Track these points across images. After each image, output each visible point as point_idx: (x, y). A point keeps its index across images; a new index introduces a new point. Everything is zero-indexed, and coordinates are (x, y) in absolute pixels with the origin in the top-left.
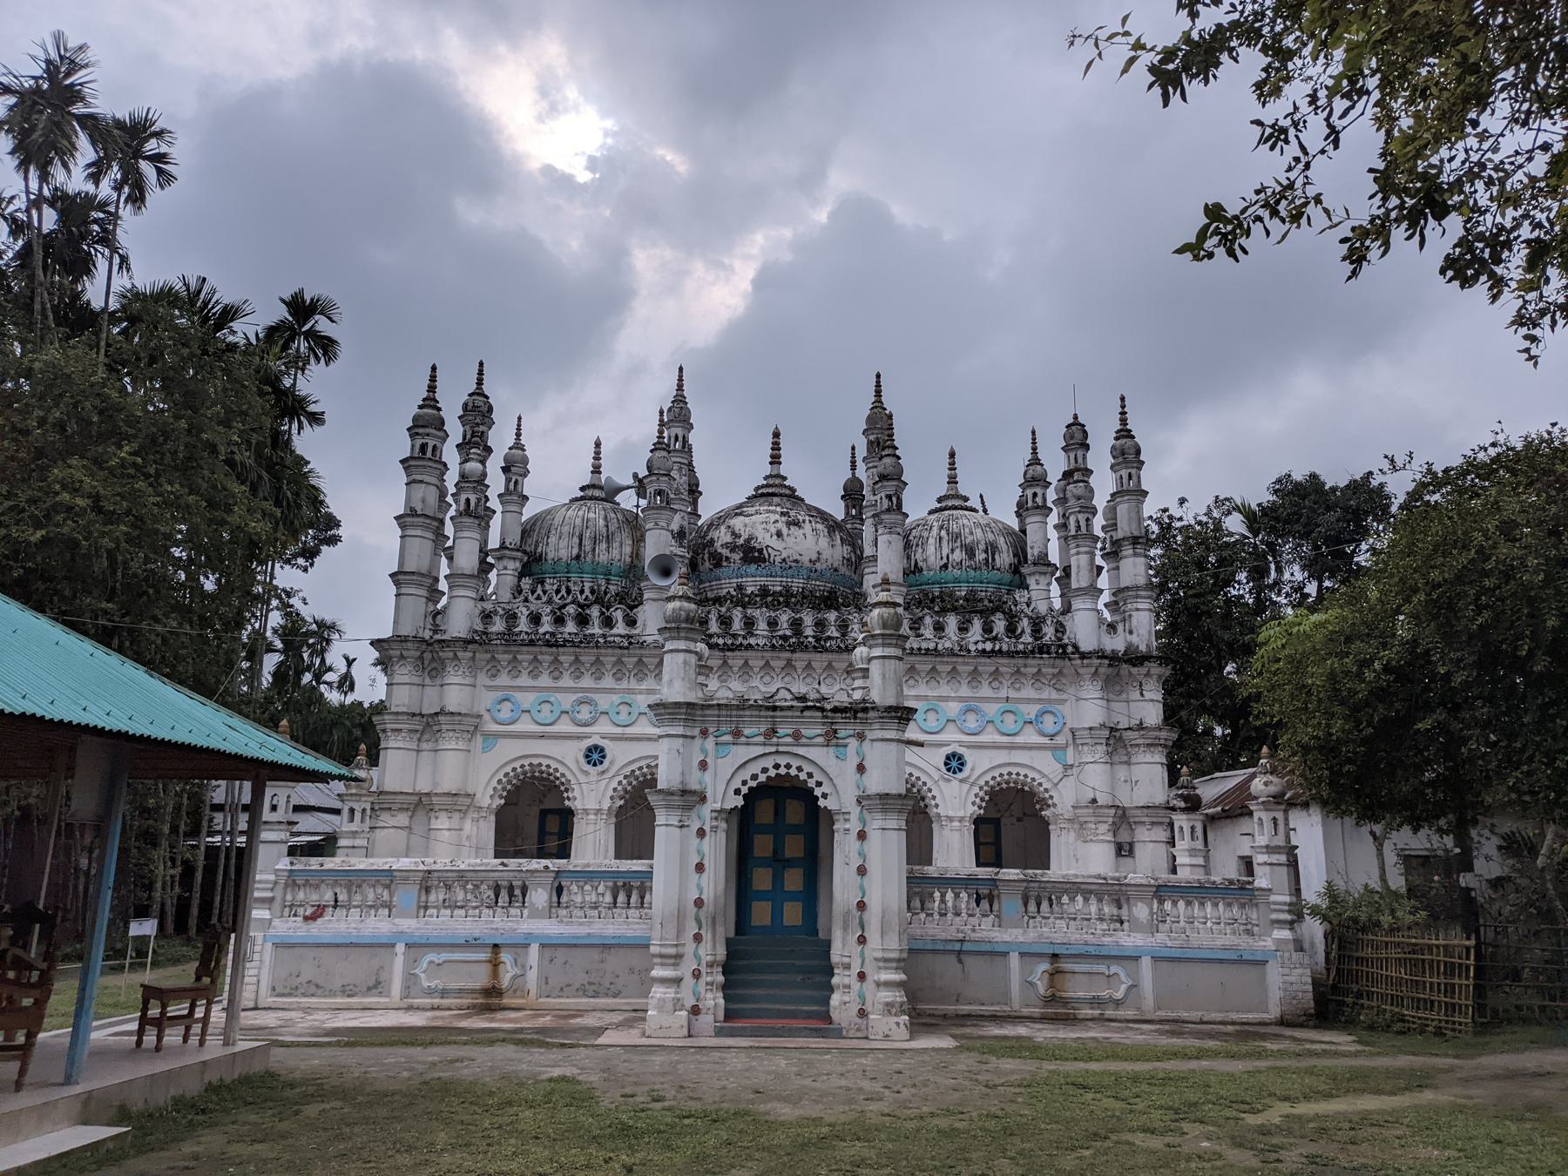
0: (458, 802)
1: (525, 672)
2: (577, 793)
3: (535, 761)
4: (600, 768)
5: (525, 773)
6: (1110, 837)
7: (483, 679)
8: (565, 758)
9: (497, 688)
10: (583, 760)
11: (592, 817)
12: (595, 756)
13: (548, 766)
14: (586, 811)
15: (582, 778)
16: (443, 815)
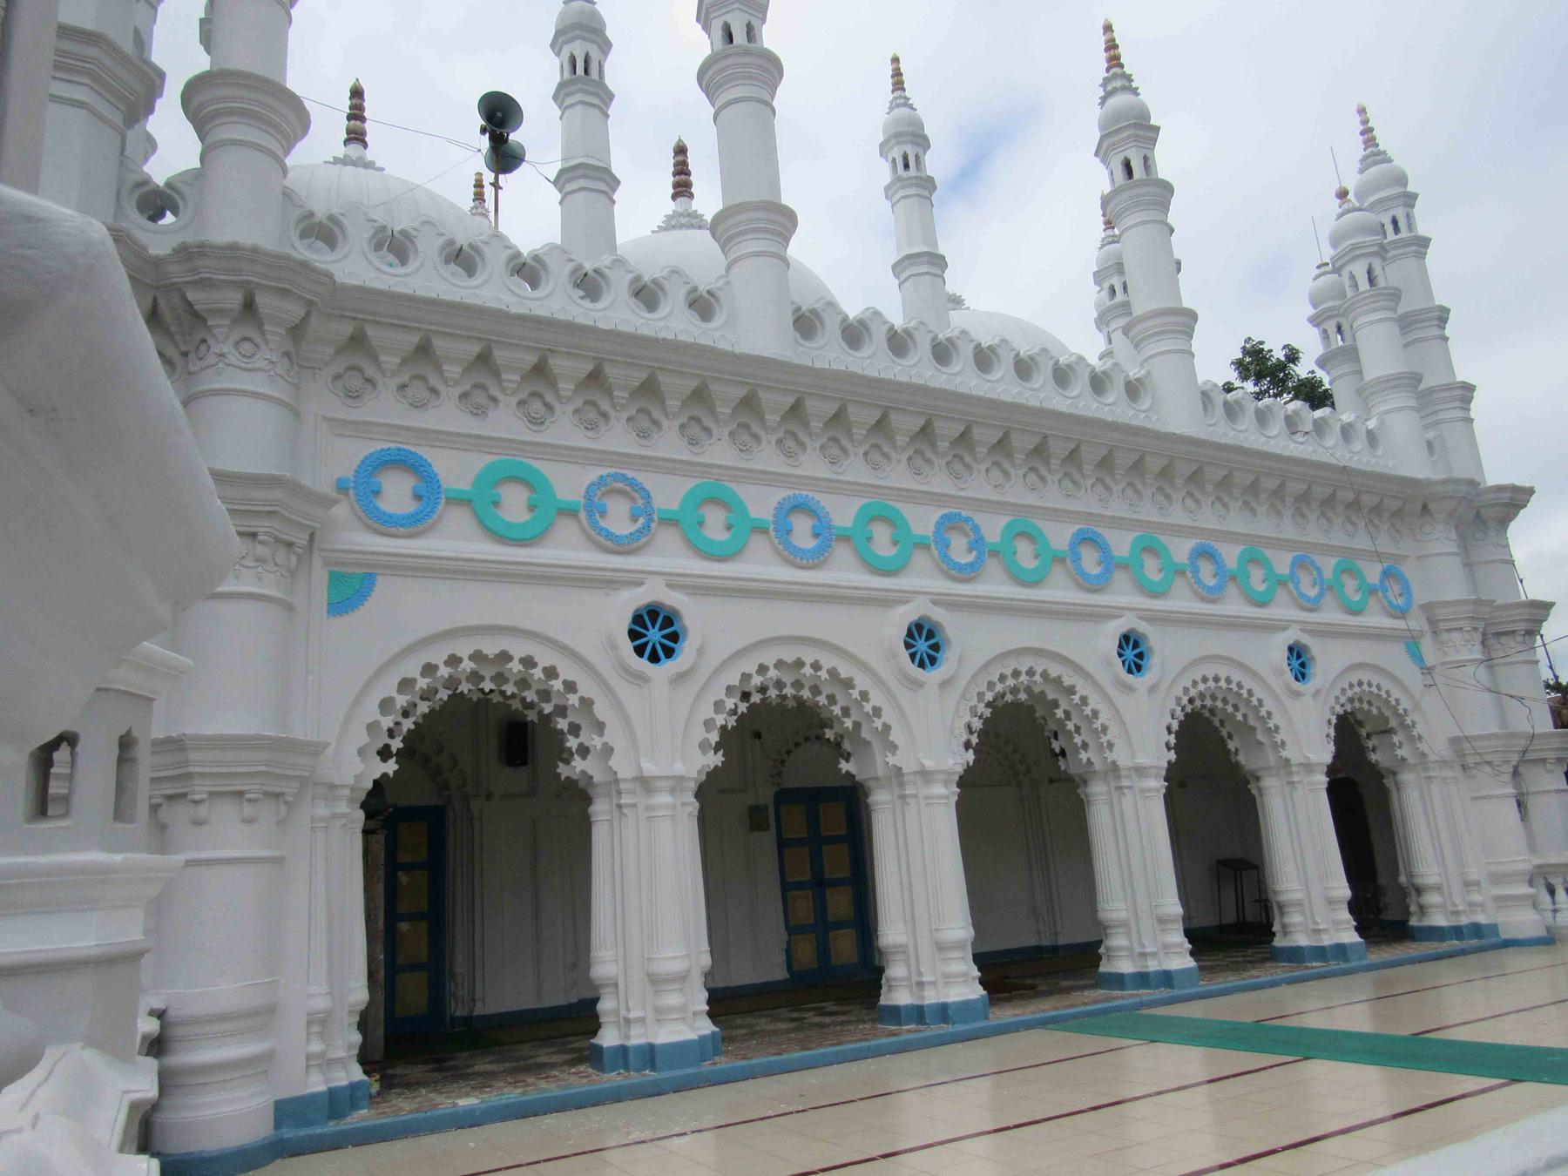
0: (270, 777)
1: (450, 394)
2: (614, 735)
3: (491, 648)
4: (668, 667)
5: (524, 683)
6: (1511, 790)
7: (322, 400)
8: (566, 634)
9: (362, 429)
10: (627, 646)
11: (663, 799)
12: (654, 635)
13: (528, 662)
14: (646, 783)
15: (625, 691)
16: (225, 816)
